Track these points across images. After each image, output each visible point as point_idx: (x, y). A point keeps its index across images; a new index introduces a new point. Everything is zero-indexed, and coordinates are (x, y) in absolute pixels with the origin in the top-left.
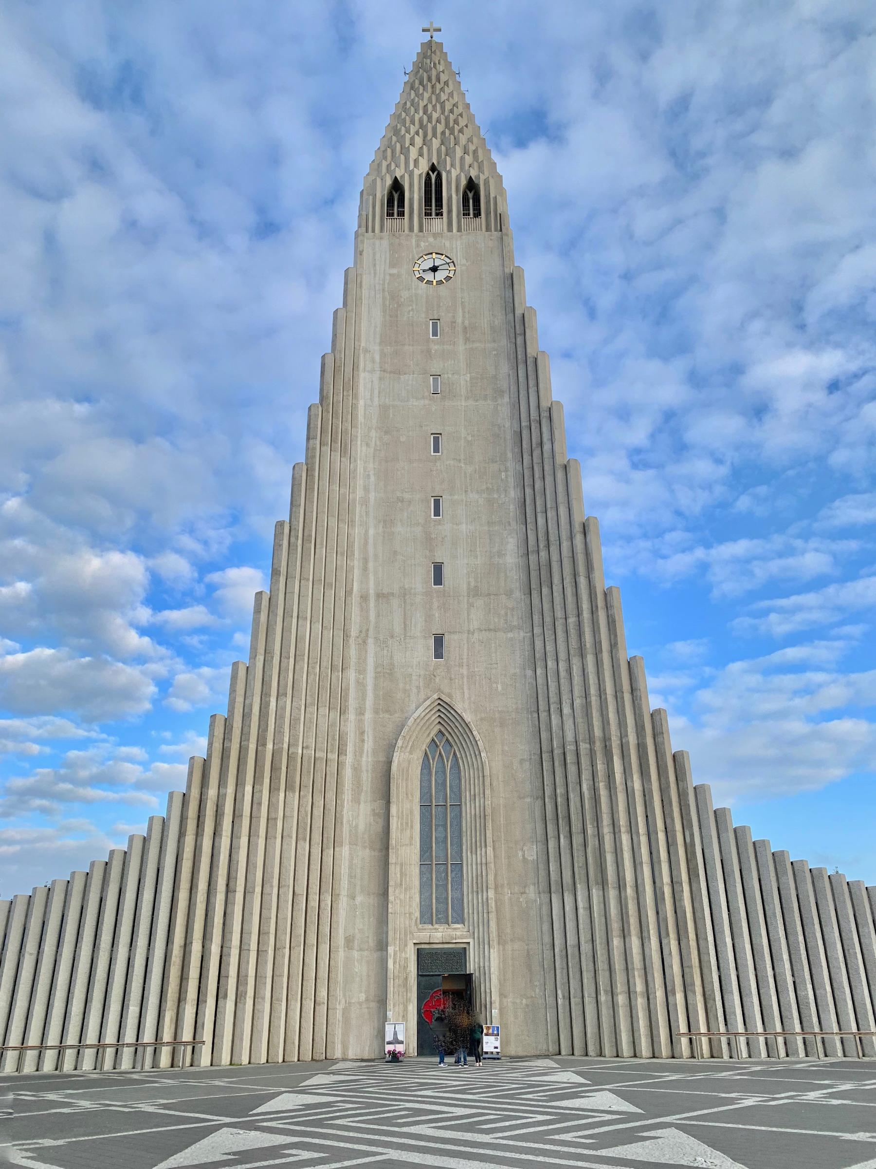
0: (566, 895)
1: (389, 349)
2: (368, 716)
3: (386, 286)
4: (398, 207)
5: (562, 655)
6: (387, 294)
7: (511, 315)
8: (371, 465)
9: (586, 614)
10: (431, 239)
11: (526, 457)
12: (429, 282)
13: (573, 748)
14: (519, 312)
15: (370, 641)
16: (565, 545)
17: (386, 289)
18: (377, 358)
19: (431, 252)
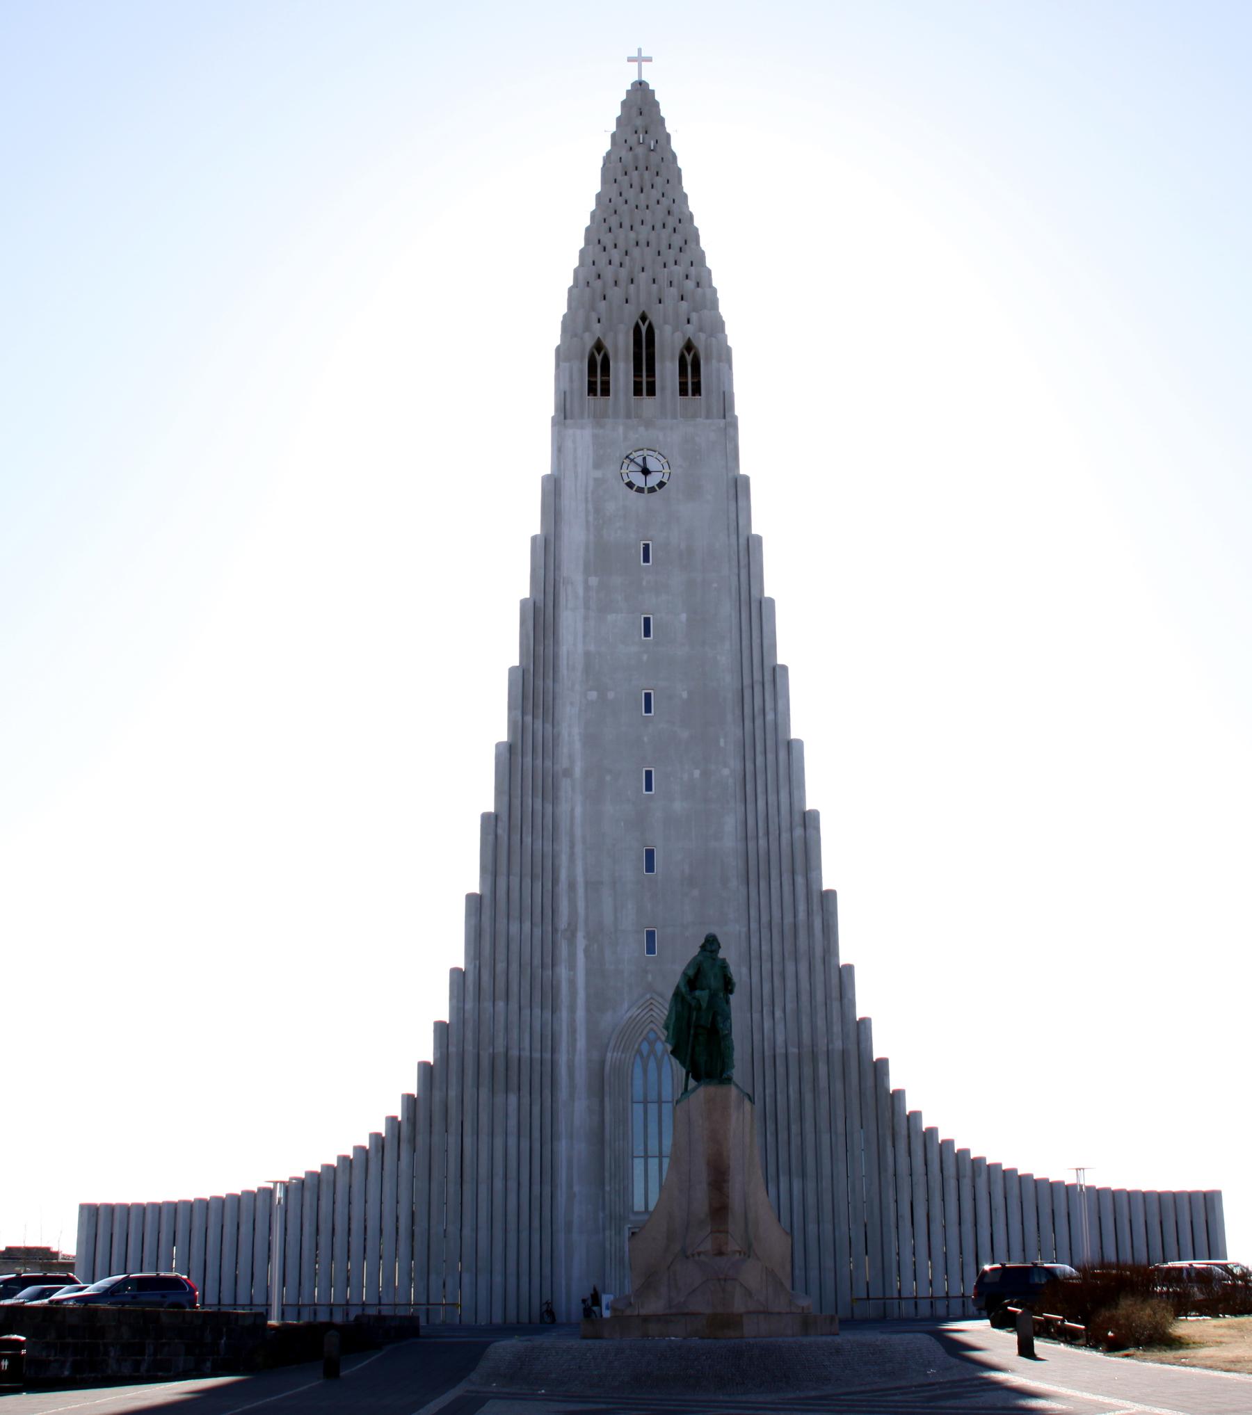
0: (770, 1185)
1: (593, 581)
2: (581, 1014)
3: (589, 495)
4: (602, 375)
5: (777, 958)
6: (590, 506)
7: (734, 537)
8: (576, 731)
9: (802, 915)
10: (642, 429)
11: (748, 723)
12: (640, 490)
13: (783, 1051)
14: (742, 541)
15: (580, 935)
16: (785, 836)
17: (590, 499)
18: (581, 592)
19: (641, 448)
